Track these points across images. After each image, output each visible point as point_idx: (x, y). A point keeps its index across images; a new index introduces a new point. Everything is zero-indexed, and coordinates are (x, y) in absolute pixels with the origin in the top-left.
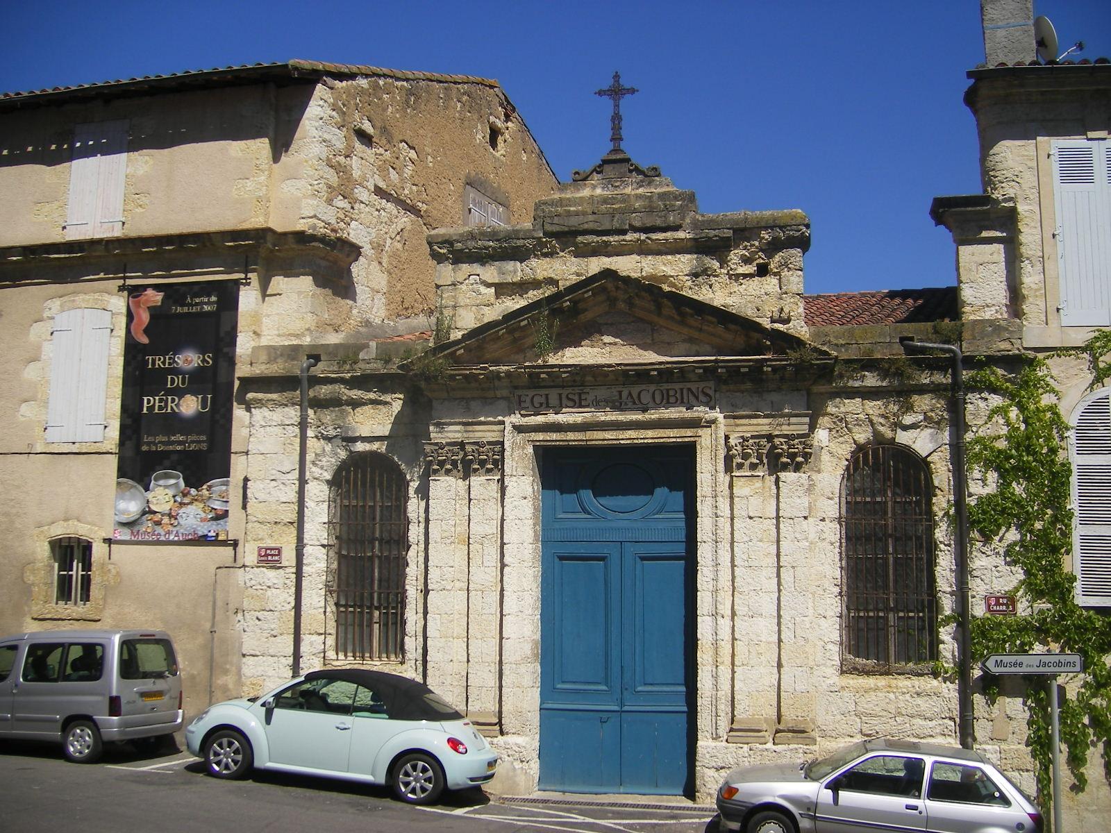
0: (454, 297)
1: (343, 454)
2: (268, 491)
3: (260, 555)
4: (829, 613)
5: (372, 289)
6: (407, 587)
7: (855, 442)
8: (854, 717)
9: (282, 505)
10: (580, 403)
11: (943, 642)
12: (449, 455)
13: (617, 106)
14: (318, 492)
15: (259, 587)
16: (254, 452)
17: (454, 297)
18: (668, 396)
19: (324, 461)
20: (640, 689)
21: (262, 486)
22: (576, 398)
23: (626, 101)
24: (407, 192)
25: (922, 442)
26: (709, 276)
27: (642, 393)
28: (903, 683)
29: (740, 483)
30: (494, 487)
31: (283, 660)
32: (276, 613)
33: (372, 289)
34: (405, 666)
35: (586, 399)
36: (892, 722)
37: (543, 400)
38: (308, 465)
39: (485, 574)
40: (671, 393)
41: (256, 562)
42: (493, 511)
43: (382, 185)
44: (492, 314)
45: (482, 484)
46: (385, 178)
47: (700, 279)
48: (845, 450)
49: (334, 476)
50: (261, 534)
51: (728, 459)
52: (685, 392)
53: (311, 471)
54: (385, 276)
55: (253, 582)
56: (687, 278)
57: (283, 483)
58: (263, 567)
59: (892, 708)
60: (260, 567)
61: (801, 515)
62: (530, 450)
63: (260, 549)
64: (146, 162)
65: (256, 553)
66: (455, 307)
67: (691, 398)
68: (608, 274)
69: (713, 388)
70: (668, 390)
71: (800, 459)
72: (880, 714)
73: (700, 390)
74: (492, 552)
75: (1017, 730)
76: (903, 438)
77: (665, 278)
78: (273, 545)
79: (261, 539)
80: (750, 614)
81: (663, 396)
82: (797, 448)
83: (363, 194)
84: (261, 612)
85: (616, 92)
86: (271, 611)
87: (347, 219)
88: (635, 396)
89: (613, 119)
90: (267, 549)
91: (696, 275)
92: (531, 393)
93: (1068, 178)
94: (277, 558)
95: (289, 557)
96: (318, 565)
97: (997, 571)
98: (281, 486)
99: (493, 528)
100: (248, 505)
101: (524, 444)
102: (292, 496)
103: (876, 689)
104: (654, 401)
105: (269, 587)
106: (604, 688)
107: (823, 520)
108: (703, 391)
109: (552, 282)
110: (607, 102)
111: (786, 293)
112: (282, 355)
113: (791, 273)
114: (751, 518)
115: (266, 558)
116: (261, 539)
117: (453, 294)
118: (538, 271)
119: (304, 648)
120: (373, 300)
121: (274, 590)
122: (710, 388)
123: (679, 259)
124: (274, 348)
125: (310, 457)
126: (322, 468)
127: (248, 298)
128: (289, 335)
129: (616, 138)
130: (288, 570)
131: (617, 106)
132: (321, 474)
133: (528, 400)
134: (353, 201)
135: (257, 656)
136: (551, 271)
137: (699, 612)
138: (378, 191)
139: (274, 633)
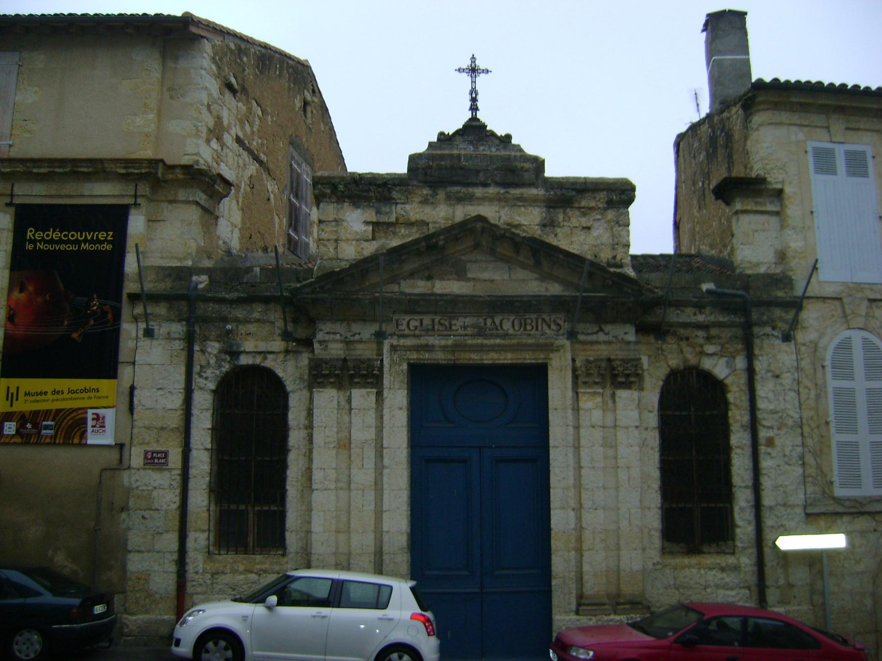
0: (336, 232)
1: (226, 367)
2: (155, 399)
3: (146, 457)
4: (653, 505)
5: (232, 223)
6: (288, 487)
7: (669, 366)
8: (673, 590)
9: (169, 412)
10: (451, 328)
11: (739, 527)
12: (333, 370)
13: (474, 82)
14: (203, 401)
15: (145, 488)
16: (141, 362)
17: (336, 232)
18: (525, 324)
19: (209, 373)
20: (497, 573)
21: (148, 394)
22: (447, 323)
23: (481, 79)
24: (255, 144)
25: (719, 369)
26: (554, 226)
27: (504, 321)
28: (709, 560)
29: (584, 398)
30: (373, 398)
31: (168, 555)
32: (162, 512)
33: (232, 223)
34: (285, 559)
35: (455, 325)
36: (703, 593)
37: (417, 324)
38: (195, 376)
39: (363, 476)
40: (529, 321)
41: (142, 464)
42: (371, 418)
43: (241, 134)
44: (369, 249)
45: (362, 397)
46: (242, 128)
47: (548, 229)
48: (662, 372)
49: (217, 387)
50: (147, 438)
51: (575, 377)
52: (540, 321)
53: (198, 381)
54: (240, 213)
55: (139, 483)
56: (537, 227)
57: (169, 392)
58: (150, 469)
59: (702, 581)
60: (146, 469)
61: (633, 425)
62: (405, 366)
63: (146, 453)
64: (35, 93)
65: (142, 457)
66: (336, 241)
67: (545, 327)
68: (480, 218)
69: (563, 319)
70: (525, 320)
71: (632, 379)
72: (694, 586)
73: (552, 320)
74: (370, 453)
75: (796, 595)
76: (707, 364)
77: (518, 226)
78: (159, 449)
79: (148, 443)
80: (594, 507)
81: (521, 323)
82: (630, 370)
83: (228, 139)
84: (147, 511)
85: (473, 71)
86: (158, 510)
87: (218, 159)
88: (498, 323)
89: (471, 93)
90: (153, 453)
91: (544, 226)
92: (407, 318)
93: (819, 170)
94: (163, 461)
95: (175, 458)
96: (202, 467)
97: (780, 470)
98: (168, 395)
99: (371, 434)
100: (135, 411)
101: (400, 361)
102: (178, 401)
103: (689, 567)
104: (514, 329)
105: (155, 488)
106: (466, 573)
107: (646, 429)
108: (554, 321)
109: (424, 223)
110: (466, 79)
111: (617, 244)
112: (170, 275)
113: (621, 228)
114: (593, 427)
115: (152, 461)
116: (148, 443)
117: (335, 229)
118: (412, 214)
119: (190, 544)
120: (232, 233)
121: (160, 491)
122: (561, 319)
123: (531, 211)
124: (163, 268)
125: (196, 369)
126: (206, 378)
127: (136, 224)
128: (172, 257)
129: (474, 108)
130: (174, 472)
131: (474, 82)
132: (205, 385)
133: (405, 323)
134: (223, 145)
135: (142, 552)
136: (423, 214)
137: (552, 506)
138: (239, 140)
139: (160, 530)
